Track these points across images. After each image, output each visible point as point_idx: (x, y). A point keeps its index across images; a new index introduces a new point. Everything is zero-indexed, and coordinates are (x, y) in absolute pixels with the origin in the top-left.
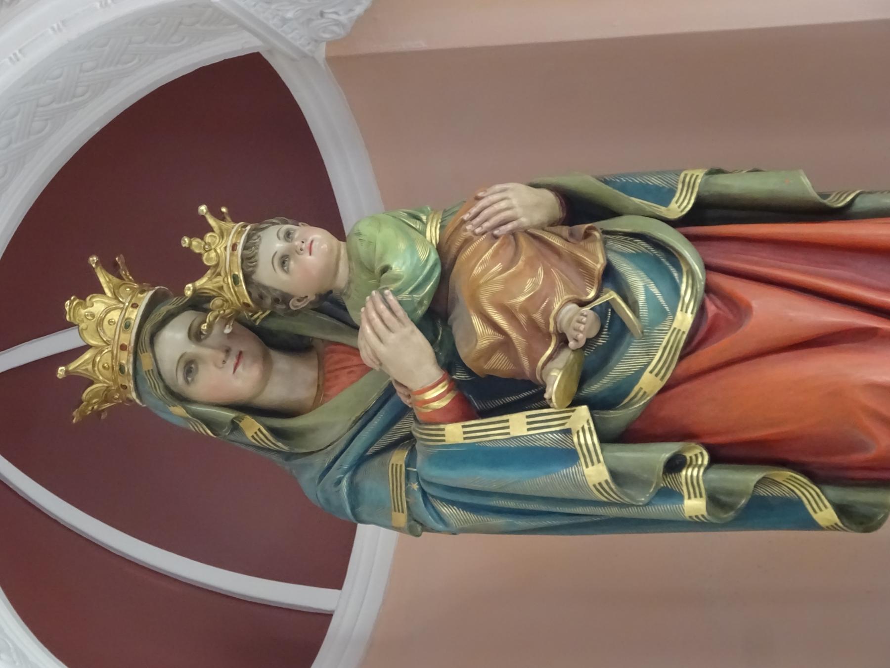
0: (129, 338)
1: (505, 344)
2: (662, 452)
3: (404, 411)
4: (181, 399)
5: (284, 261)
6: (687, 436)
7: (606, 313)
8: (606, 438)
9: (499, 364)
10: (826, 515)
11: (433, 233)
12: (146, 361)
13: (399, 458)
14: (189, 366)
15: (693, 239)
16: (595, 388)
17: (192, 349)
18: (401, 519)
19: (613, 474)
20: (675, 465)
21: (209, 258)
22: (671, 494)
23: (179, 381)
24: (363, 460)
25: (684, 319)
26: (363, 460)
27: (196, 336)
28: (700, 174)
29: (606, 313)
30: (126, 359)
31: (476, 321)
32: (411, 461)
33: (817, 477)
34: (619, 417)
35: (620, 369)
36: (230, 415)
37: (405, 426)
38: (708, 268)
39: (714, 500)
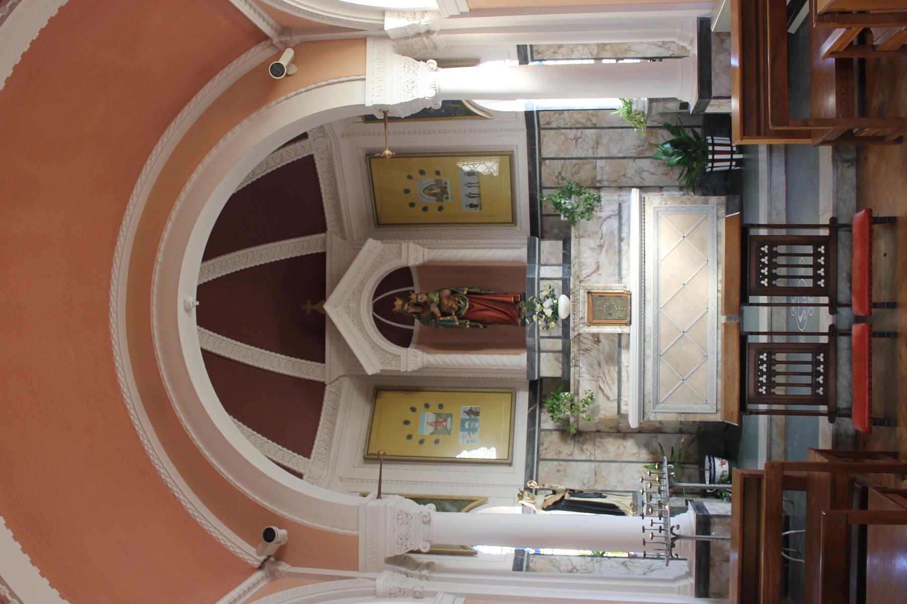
0: (401, 306)
1: (447, 309)
2: (464, 321)
3: (434, 315)
4: (407, 312)
5: (421, 299)
6: (469, 319)
7: (459, 307)
8: (459, 319)
9: (447, 311)
10: (482, 327)
11: (438, 295)
12: (403, 309)
13: (433, 320)
14: (408, 309)
15: (468, 297)
16: (457, 314)
17: (408, 307)
18: (433, 327)
19: (460, 323)
20: (466, 322)
21: (412, 298)
22: (466, 325)
23: (407, 311)
24: (429, 320)
25: (467, 307)
26: (429, 320)
27: (409, 305)
28: (467, 289)
29: (459, 307)
30: (400, 308)
31: (444, 307)
32: (435, 321)
33: (481, 323)
34: (459, 317)
35: (460, 312)
36: (411, 314)
37: (434, 317)
38: (470, 301)
39: (470, 326)
